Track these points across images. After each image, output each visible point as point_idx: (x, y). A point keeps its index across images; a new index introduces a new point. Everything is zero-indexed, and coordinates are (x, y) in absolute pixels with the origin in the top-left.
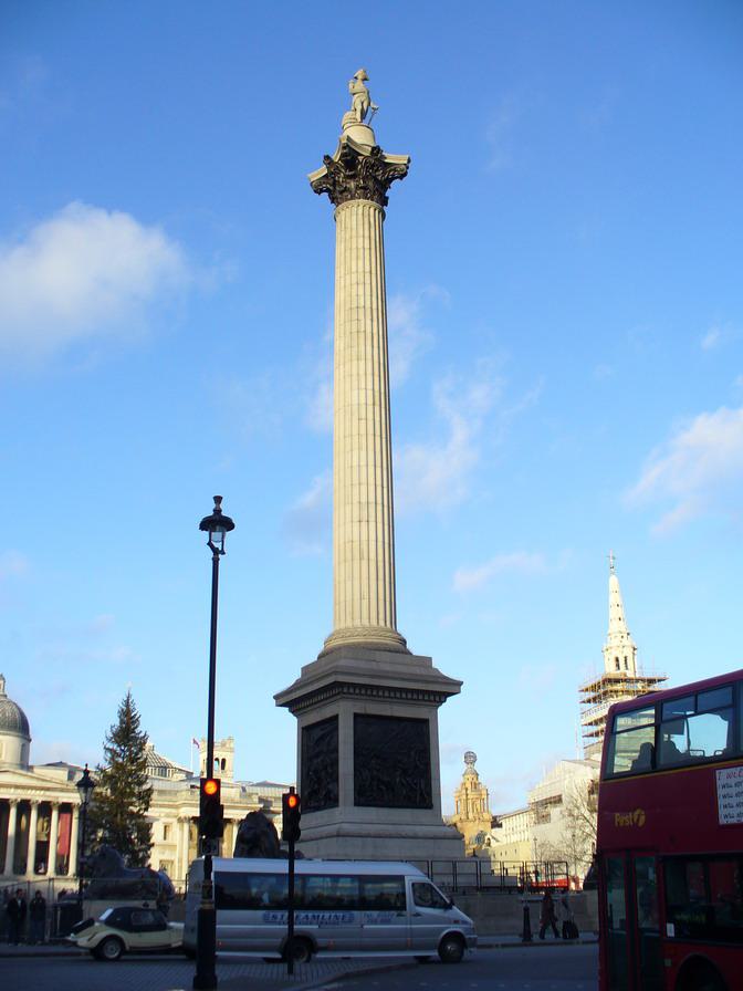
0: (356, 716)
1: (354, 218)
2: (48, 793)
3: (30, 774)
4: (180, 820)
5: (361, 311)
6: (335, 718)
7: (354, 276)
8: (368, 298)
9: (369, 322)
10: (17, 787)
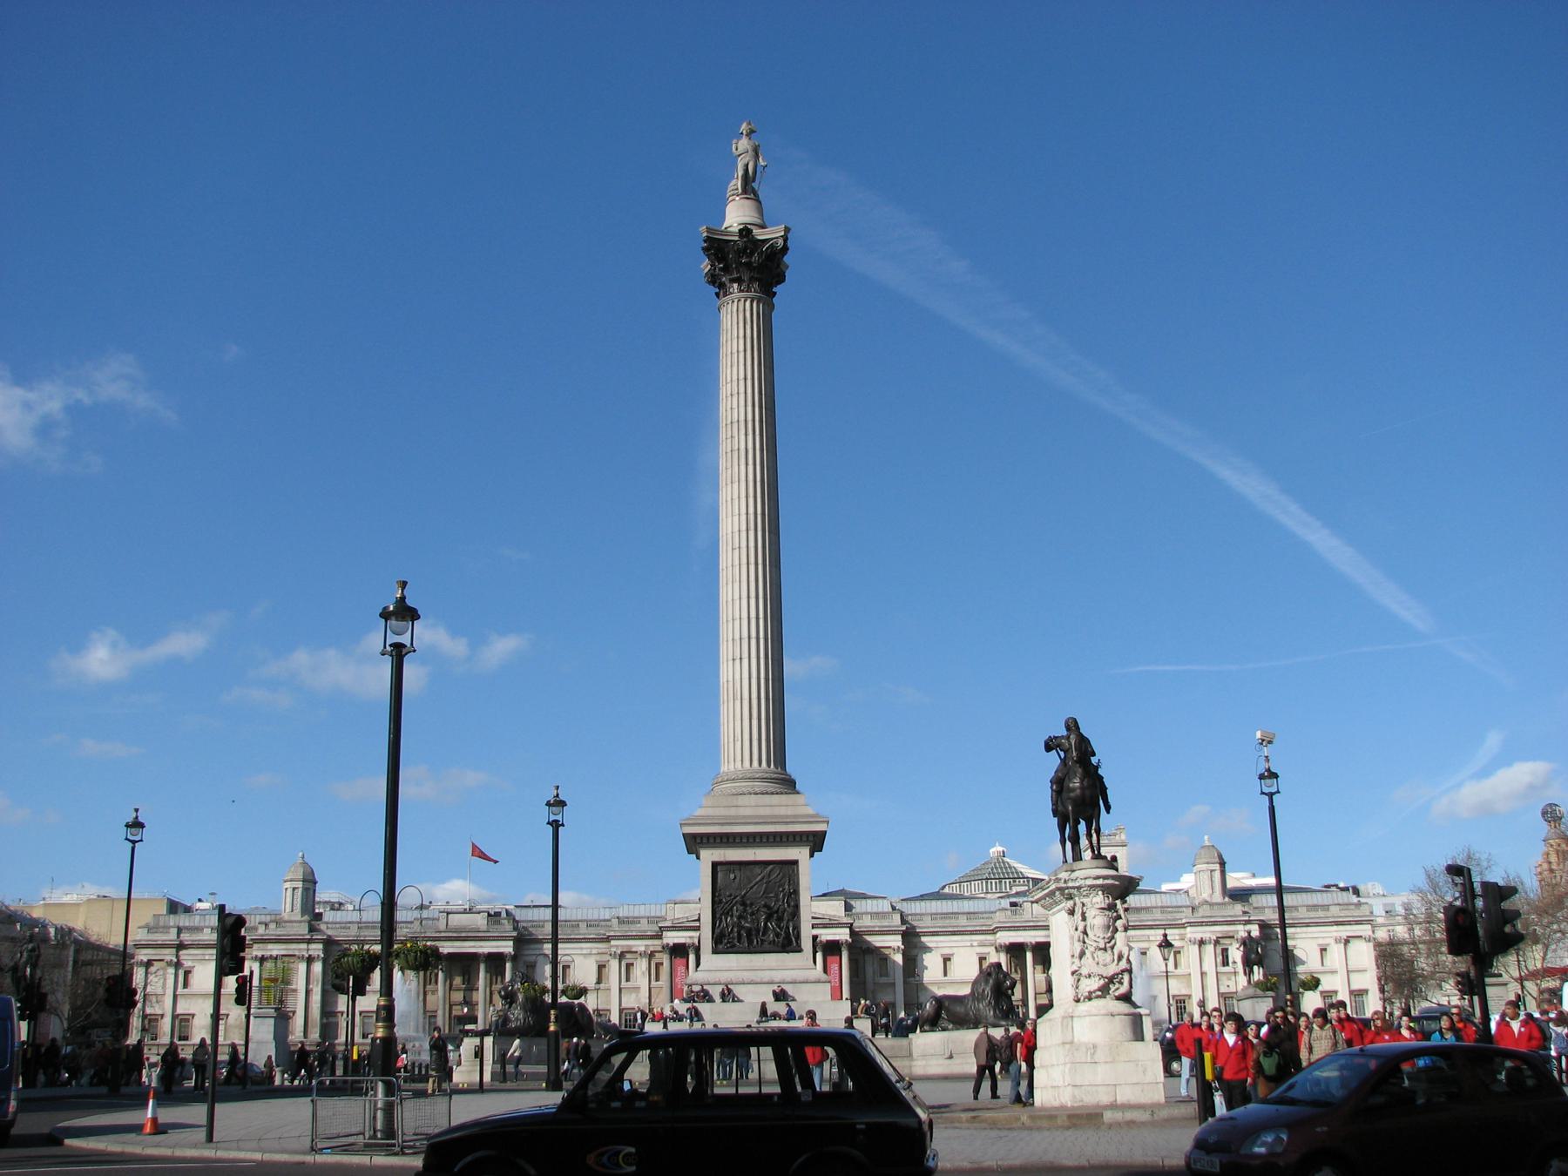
5: (735, 425)
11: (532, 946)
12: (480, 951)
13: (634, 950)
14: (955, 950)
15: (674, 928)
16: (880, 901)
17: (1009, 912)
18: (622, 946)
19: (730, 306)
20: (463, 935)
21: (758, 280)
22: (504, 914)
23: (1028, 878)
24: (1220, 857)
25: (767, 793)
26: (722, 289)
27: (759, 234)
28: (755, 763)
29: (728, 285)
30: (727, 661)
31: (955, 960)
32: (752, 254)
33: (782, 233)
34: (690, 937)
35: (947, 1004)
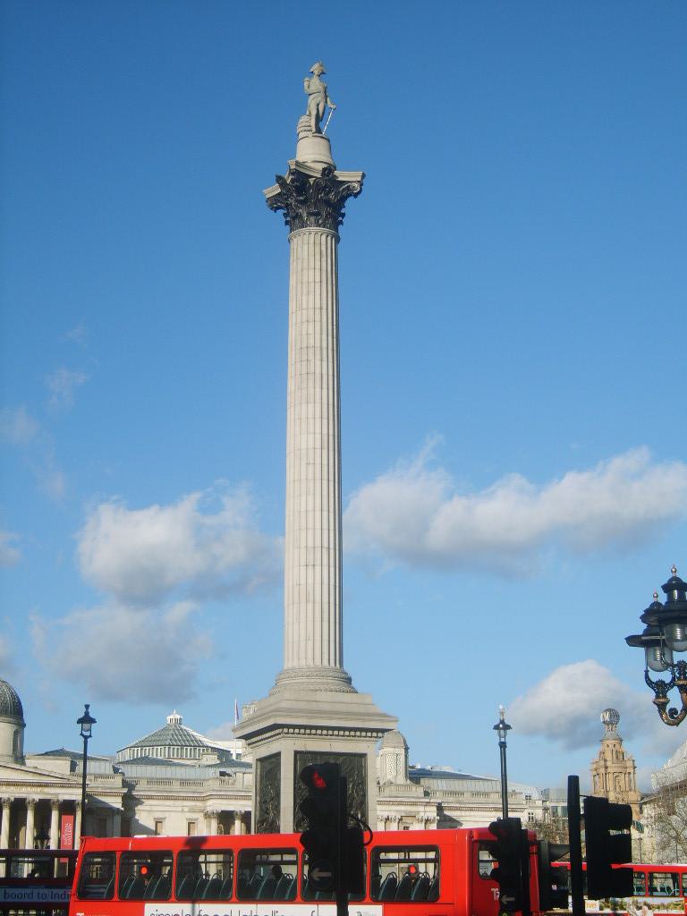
0: (296, 753)
1: (306, 247)
2: (46, 790)
3: (23, 768)
4: (207, 816)
5: (311, 351)
6: (278, 754)
8: (318, 337)
9: (318, 363)
14: (167, 815)
16: (103, 763)
17: (218, 782)
23: (207, 747)
24: (405, 741)
27: (341, 175)
28: (326, 662)
31: (166, 823)
32: (329, 192)
33: (359, 179)
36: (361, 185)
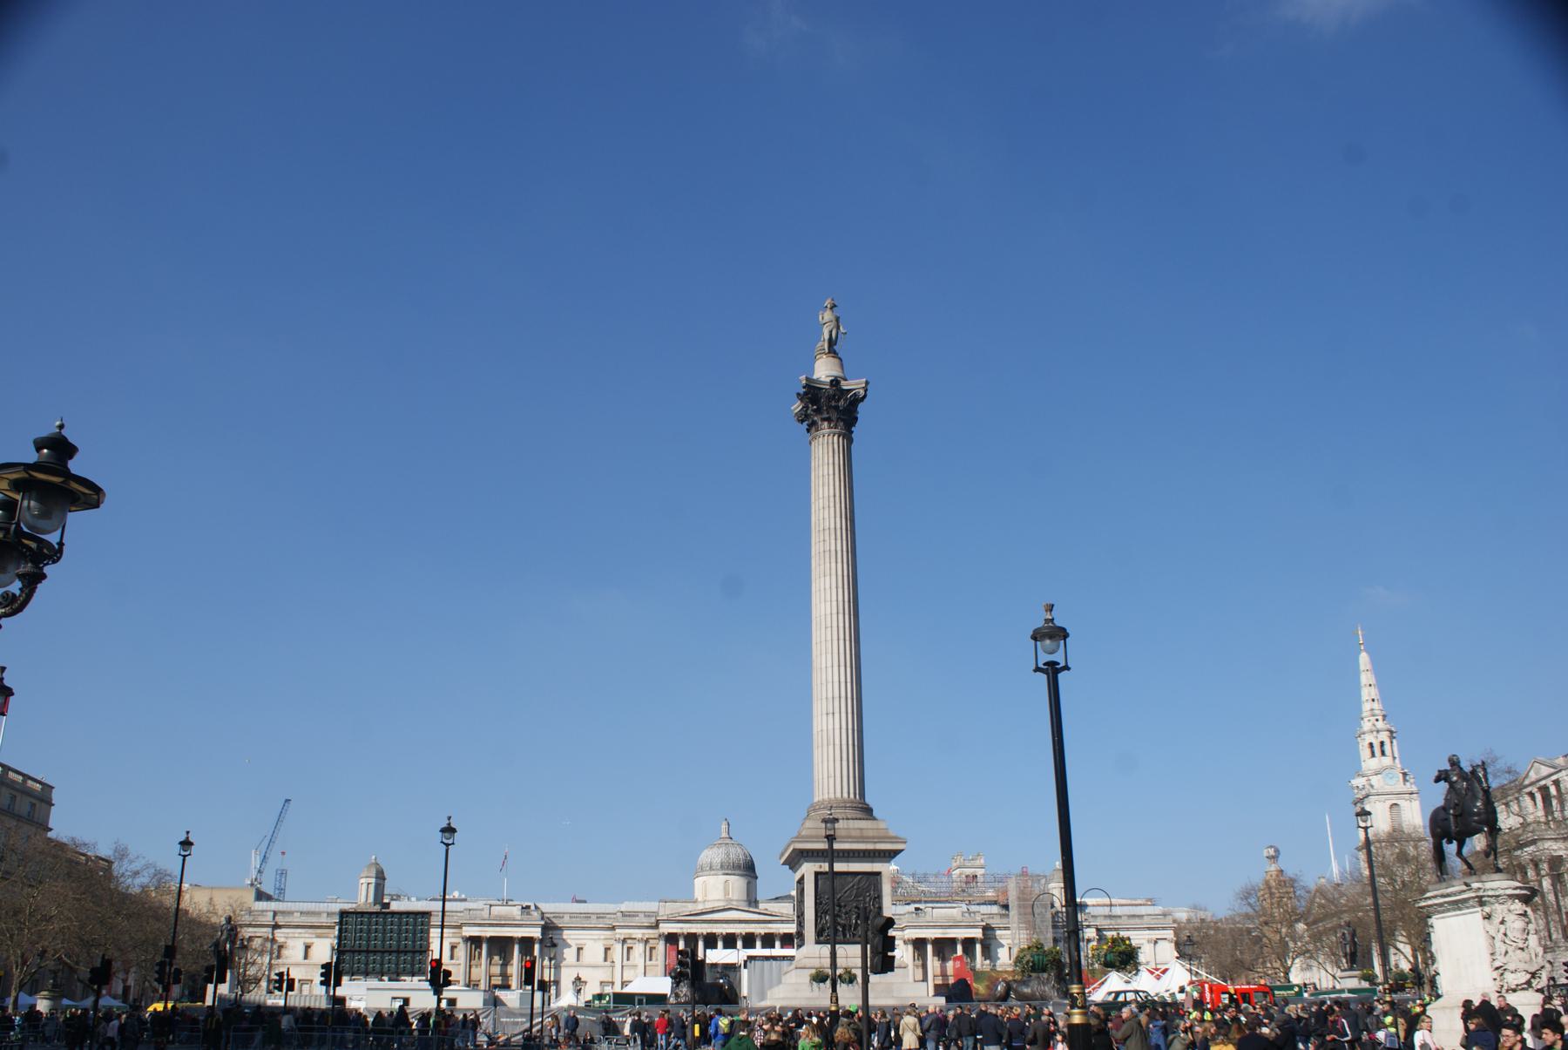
0: (817, 874)
1: (821, 447)
2: (770, 925)
7: (821, 501)
9: (833, 542)
10: (740, 922)
11: (555, 932)
12: (515, 935)
13: (634, 937)
15: (668, 921)
18: (625, 934)
19: (821, 439)
20: (503, 922)
21: (842, 420)
22: (533, 908)
25: (856, 819)
26: (812, 426)
27: (845, 386)
29: (820, 423)
30: (822, 715)
32: (839, 400)
33: (864, 385)
34: (682, 928)
35: (1015, 986)
36: (866, 391)
